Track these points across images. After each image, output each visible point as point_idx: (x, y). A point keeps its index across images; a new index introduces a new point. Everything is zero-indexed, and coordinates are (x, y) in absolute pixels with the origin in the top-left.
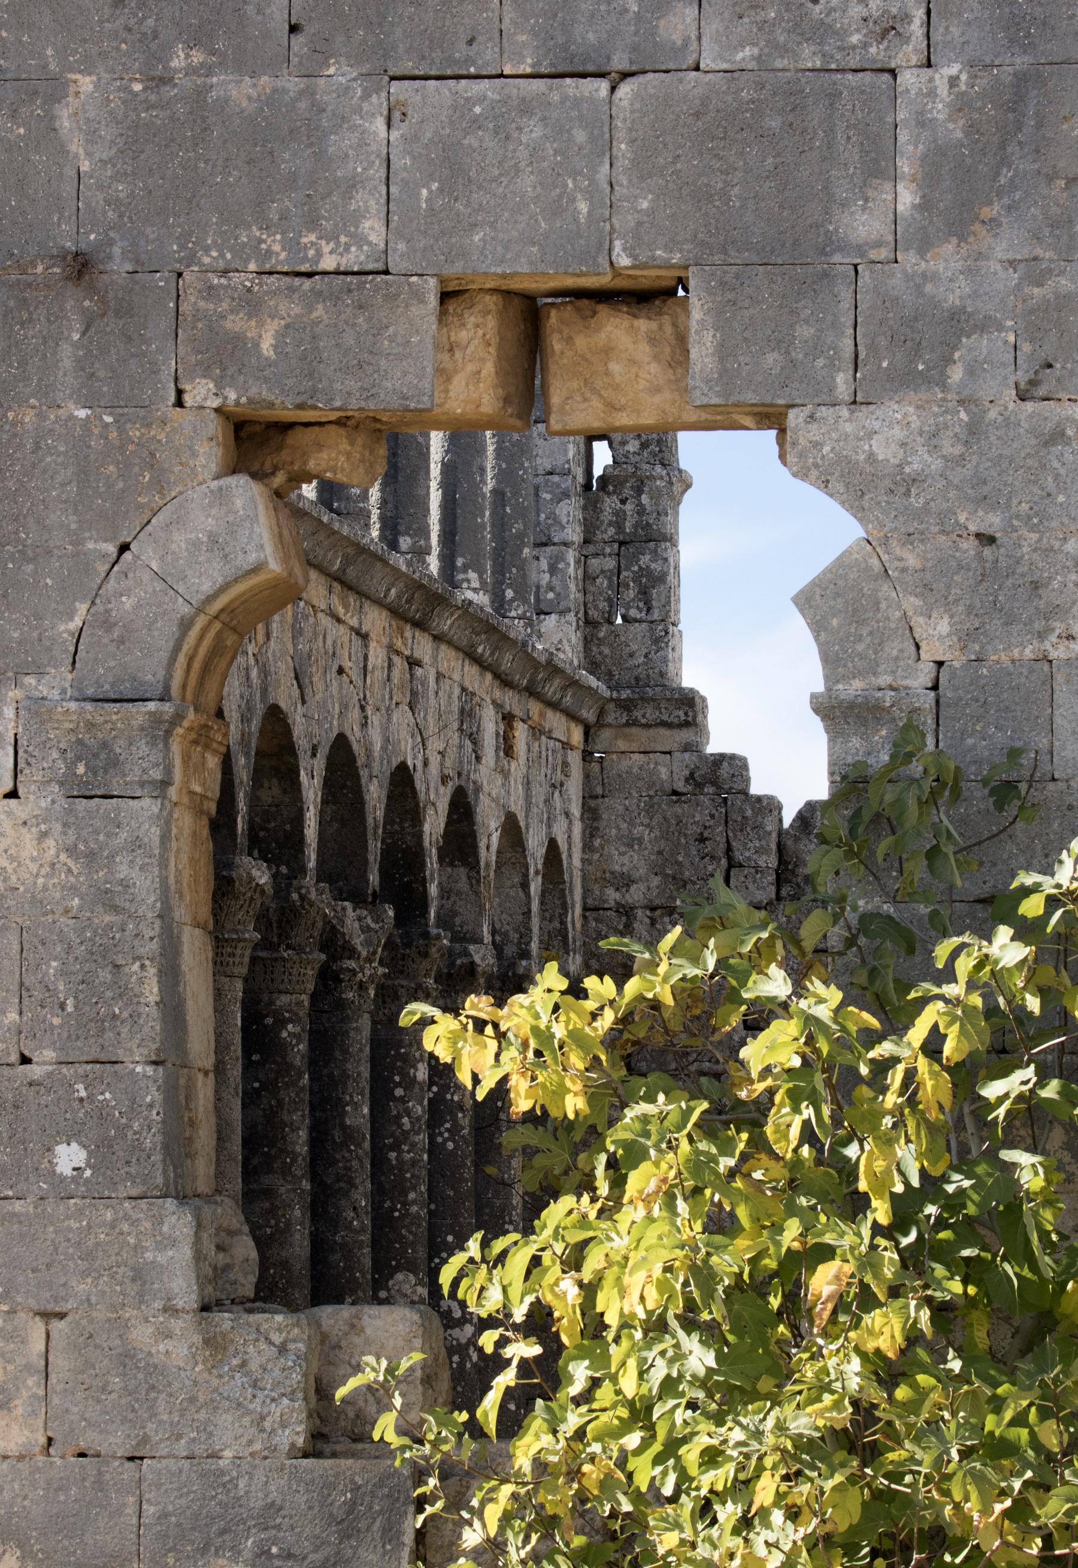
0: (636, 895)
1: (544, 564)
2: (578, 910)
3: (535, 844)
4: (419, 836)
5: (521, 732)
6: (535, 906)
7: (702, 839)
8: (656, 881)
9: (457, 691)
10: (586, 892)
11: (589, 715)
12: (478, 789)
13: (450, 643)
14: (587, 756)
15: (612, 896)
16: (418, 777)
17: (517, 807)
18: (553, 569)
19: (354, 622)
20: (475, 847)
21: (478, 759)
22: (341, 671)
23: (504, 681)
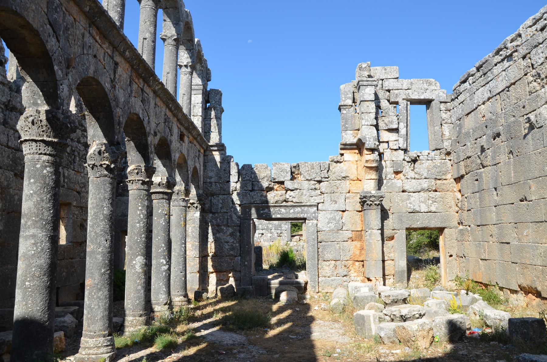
0: (213, 180)
1: (196, 119)
2: (202, 183)
3: (190, 164)
4: (147, 140)
5: (186, 139)
6: (190, 176)
7: (225, 170)
8: (216, 178)
9: (163, 113)
10: (204, 179)
11: (205, 148)
12: (171, 142)
13: (159, 97)
14: (204, 156)
15: (208, 180)
16: (145, 123)
17: (185, 152)
18: (198, 120)
19: (109, 51)
20: (171, 156)
21: (172, 135)
22: (95, 56)
23: (181, 124)
